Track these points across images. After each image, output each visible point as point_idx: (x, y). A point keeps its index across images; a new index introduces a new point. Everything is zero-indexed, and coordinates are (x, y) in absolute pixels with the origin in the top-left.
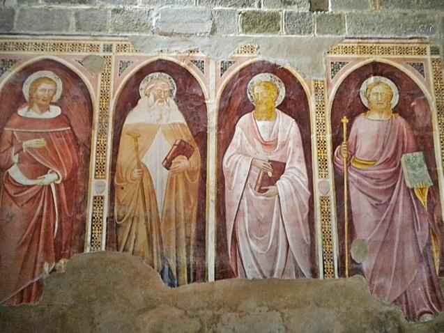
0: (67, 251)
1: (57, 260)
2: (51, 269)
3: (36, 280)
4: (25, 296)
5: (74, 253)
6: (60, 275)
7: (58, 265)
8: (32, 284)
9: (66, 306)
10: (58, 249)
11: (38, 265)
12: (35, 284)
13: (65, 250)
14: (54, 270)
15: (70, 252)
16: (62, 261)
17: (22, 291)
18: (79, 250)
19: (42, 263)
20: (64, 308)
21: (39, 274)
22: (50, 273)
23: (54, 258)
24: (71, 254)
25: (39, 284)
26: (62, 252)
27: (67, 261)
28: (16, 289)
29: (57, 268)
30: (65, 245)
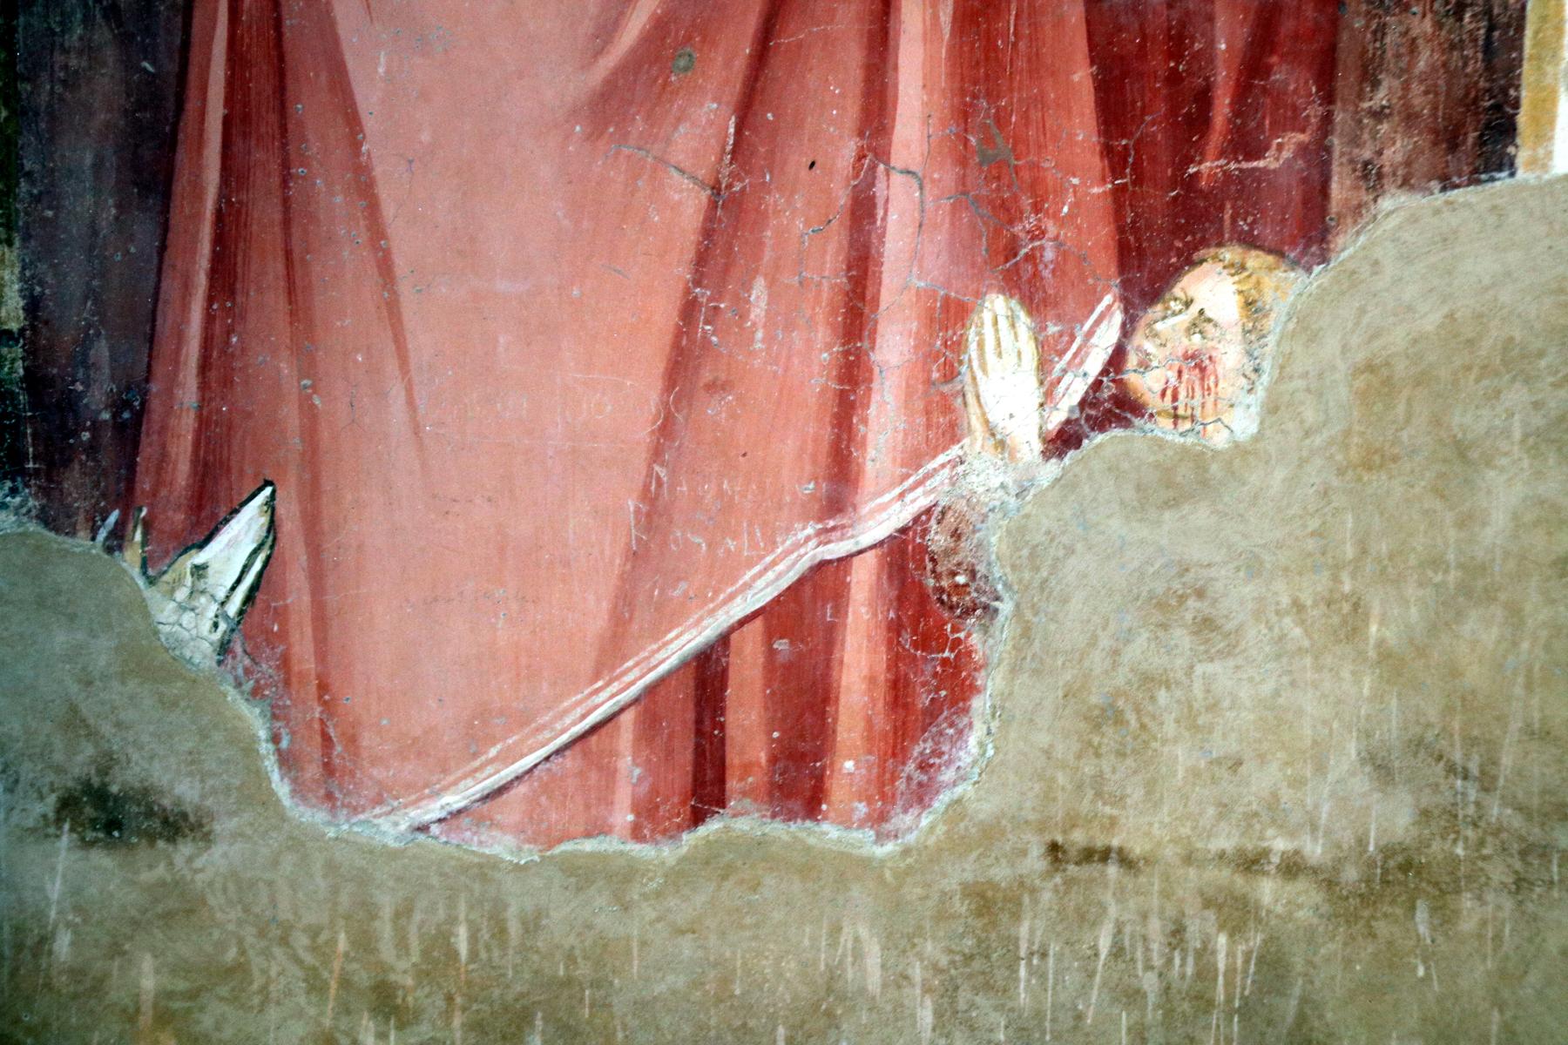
0: (1281, 155)
1: (1146, 273)
2: (1074, 390)
3: (880, 518)
4: (749, 727)
5: (1371, 177)
6: (1188, 480)
7: (1166, 331)
8: (825, 581)
9: (1292, 868)
10: (1154, 126)
11: (894, 347)
12: (864, 580)
13: (1245, 144)
14: (1112, 405)
15: (1318, 157)
16: (1212, 288)
17: (707, 673)
18: (1449, 138)
19: (948, 317)
20: (1267, 890)
21: (914, 459)
22: (1063, 441)
23: (1099, 237)
24: (1340, 189)
25: (929, 597)
26: (1208, 167)
27: (1287, 287)
28: (613, 651)
29: (1147, 383)
30: (1253, 68)
